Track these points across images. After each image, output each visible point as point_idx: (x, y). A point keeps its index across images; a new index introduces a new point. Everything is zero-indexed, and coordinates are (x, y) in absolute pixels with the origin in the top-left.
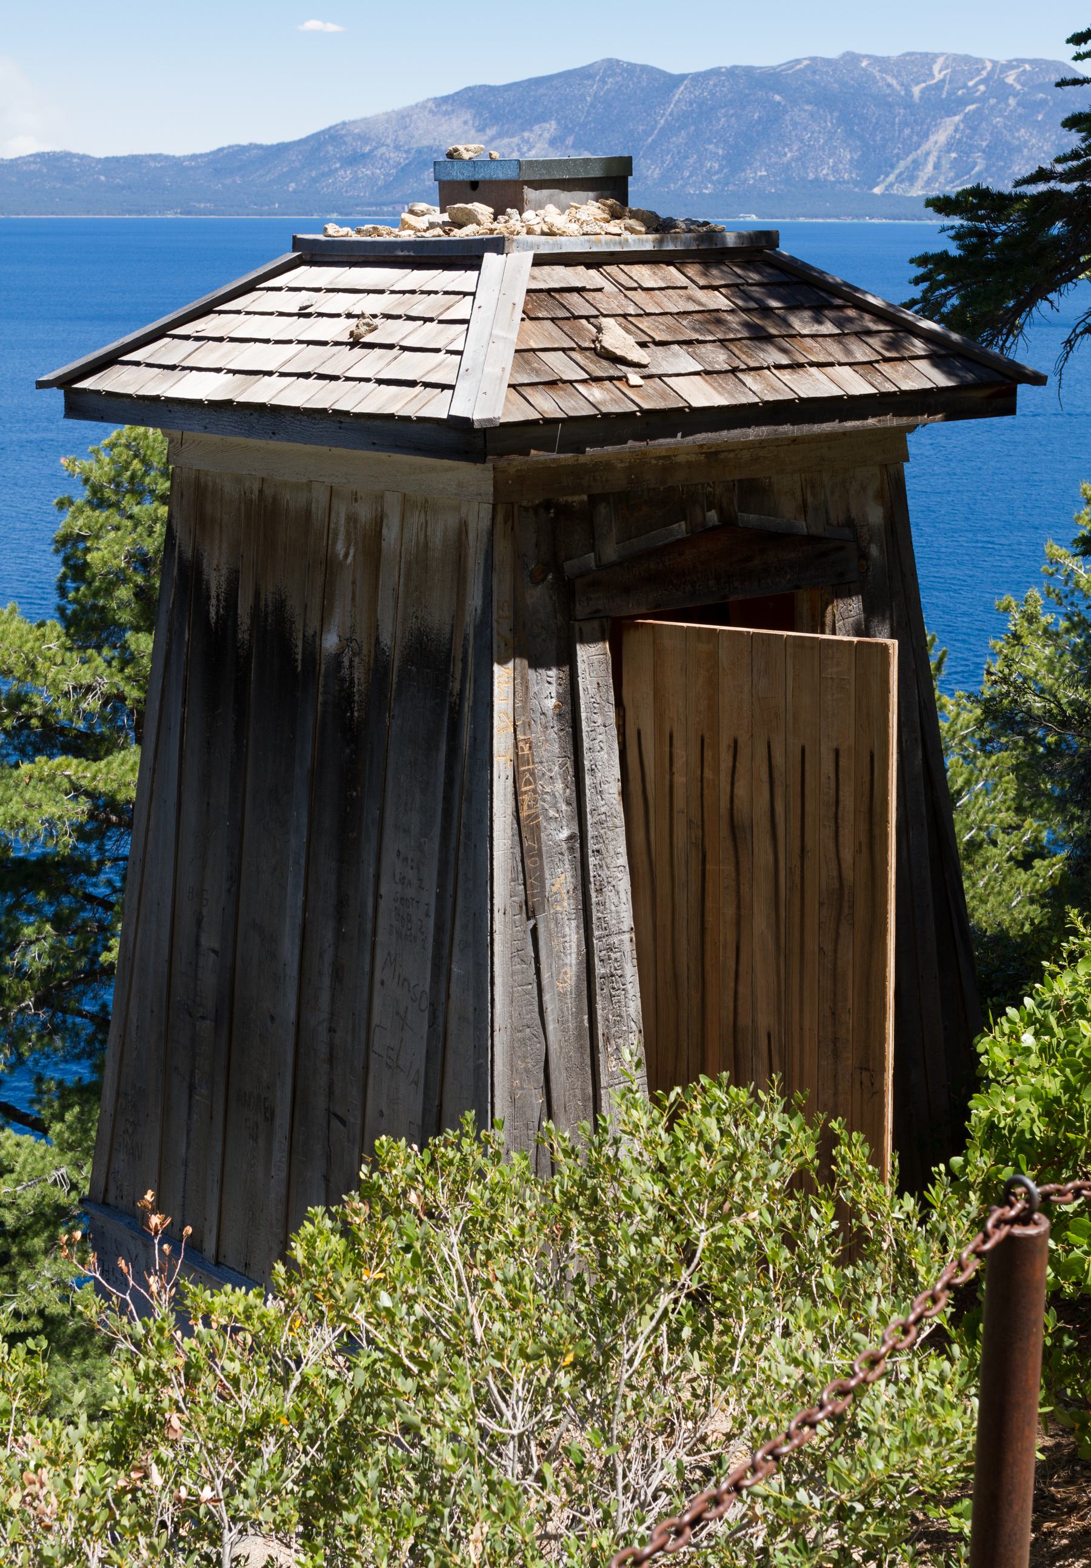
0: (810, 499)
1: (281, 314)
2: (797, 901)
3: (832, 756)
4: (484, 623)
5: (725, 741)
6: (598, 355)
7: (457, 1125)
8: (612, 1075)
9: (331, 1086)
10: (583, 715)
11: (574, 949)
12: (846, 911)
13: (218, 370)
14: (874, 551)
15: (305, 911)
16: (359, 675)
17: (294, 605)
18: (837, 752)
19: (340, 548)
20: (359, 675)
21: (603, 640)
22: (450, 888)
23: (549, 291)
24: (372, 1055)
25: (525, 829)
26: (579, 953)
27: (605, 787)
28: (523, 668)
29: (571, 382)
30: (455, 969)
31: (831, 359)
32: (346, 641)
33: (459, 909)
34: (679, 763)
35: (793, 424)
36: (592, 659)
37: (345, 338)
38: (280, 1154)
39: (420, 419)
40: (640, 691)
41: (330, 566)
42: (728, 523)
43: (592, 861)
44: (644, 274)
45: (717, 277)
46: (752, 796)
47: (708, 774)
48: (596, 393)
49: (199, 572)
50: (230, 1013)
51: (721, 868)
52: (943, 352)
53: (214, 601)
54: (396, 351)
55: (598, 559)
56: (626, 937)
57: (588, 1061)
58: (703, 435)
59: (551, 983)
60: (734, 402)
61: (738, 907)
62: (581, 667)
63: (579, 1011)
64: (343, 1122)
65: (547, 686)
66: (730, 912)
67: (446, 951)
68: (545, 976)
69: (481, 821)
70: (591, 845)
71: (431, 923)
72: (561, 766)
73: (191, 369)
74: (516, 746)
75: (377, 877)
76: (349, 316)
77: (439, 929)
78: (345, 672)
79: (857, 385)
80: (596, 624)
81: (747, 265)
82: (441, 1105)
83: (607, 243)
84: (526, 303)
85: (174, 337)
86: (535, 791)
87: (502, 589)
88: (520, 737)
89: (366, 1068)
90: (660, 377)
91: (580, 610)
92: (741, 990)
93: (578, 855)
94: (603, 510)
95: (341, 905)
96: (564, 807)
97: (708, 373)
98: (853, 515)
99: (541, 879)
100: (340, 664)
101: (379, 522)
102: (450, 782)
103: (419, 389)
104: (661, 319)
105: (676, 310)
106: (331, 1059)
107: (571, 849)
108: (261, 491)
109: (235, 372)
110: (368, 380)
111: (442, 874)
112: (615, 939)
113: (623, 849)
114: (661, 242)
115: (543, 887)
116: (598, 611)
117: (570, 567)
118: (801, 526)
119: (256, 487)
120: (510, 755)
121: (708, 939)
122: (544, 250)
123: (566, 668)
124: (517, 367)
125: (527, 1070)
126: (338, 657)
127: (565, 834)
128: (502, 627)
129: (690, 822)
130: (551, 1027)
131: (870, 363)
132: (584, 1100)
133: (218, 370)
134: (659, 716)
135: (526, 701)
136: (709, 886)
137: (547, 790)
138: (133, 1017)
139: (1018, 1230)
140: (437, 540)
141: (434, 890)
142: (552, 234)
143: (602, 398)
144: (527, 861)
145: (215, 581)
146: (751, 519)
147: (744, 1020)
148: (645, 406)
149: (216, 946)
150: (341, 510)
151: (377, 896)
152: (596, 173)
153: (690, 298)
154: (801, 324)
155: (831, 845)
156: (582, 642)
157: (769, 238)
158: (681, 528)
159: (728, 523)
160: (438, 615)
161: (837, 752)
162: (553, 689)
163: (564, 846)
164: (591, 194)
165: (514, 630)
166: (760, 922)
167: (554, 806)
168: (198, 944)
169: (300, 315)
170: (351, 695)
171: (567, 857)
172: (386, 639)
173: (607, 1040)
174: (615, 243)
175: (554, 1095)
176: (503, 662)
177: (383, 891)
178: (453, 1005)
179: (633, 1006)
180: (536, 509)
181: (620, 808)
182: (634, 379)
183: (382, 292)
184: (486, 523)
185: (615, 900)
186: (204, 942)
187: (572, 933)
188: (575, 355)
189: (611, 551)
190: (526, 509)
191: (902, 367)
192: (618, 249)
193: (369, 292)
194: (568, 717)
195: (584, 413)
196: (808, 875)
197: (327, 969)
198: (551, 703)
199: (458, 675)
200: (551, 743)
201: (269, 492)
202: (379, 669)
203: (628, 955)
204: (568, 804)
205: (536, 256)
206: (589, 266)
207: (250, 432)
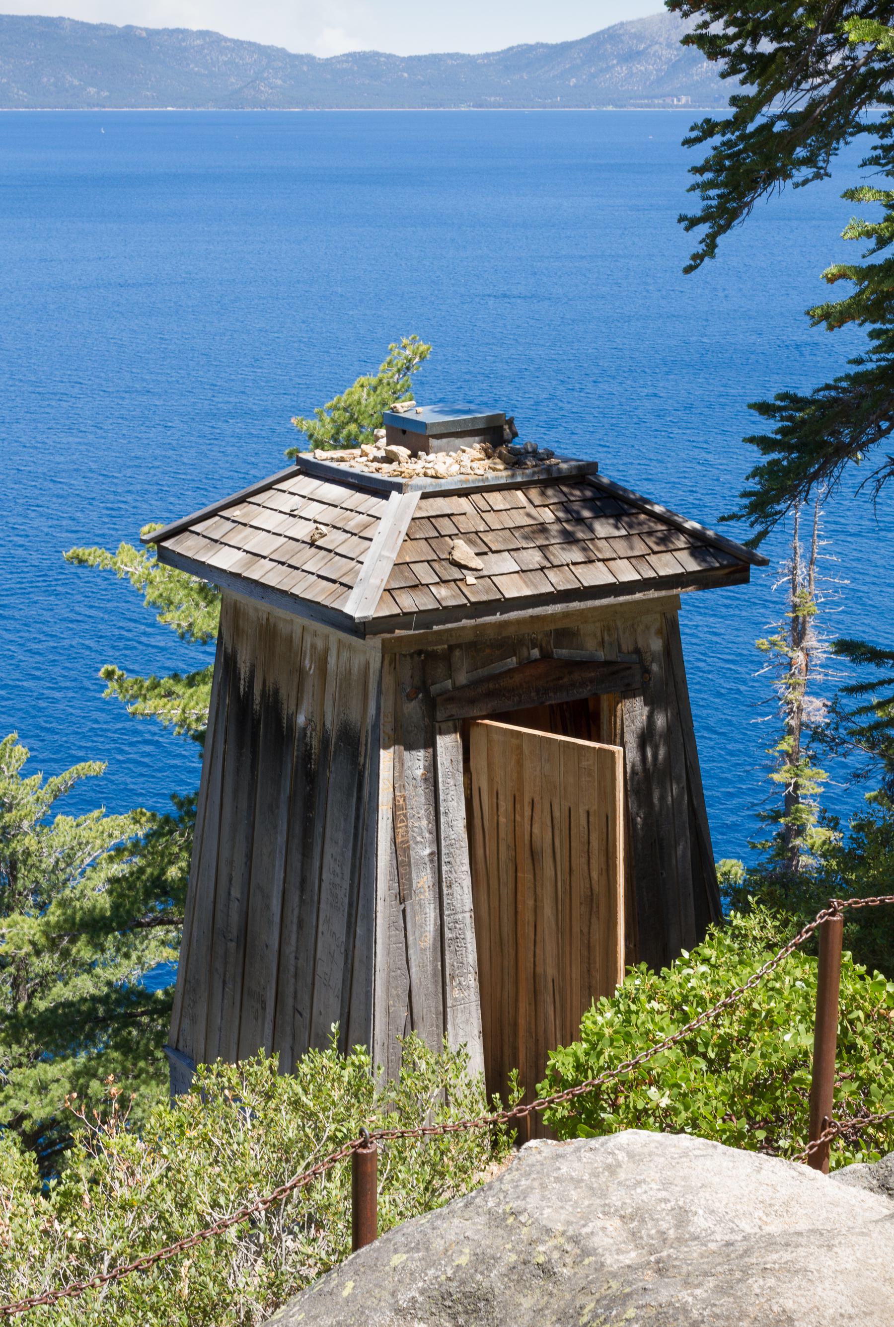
0: (606, 638)
1: (281, 512)
2: (568, 901)
3: (585, 815)
4: (376, 726)
5: (527, 800)
6: (451, 563)
7: (255, 1054)
8: (455, 999)
9: (296, 992)
10: (440, 780)
11: (432, 922)
12: (595, 909)
13: (239, 549)
14: (655, 667)
15: (284, 882)
16: (315, 743)
17: (283, 692)
18: (588, 813)
19: (307, 663)
20: (315, 743)
21: (455, 732)
22: (356, 881)
23: (428, 518)
24: (317, 977)
25: (400, 849)
26: (435, 924)
27: (454, 823)
28: (400, 752)
29: (427, 585)
30: (358, 931)
31: (615, 556)
32: (309, 721)
33: (361, 894)
34: (502, 810)
35: (580, 601)
36: (448, 745)
37: (308, 540)
38: (268, 1030)
39: (333, 608)
40: (479, 762)
41: (301, 672)
42: (546, 656)
43: (444, 868)
44: (497, 500)
45: (552, 496)
46: (542, 834)
47: (518, 818)
48: (442, 592)
49: (235, 663)
50: (245, 938)
51: (526, 876)
52: (699, 544)
53: (242, 682)
54: (332, 554)
55: (454, 683)
56: (468, 915)
57: (440, 990)
58: (515, 613)
59: (415, 944)
60: (536, 592)
61: (535, 900)
62: (439, 750)
63: (435, 959)
64: (301, 1015)
65: (417, 761)
66: (531, 903)
67: (353, 920)
68: (411, 939)
69: (372, 844)
70: (444, 858)
71: (346, 900)
72: (426, 810)
73: (226, 544)
74: (394, 799)
75: (321, 868)
76: (315, 522)
77: (350, 905)
78: (308, 739)
79: (627, 574)
80: (450, 724)
81: (573, 486)
82: (349, 1012)
83: (473, 481)
84: (410, 528)
85: (222, 517)
86: (407, 826)
87: (388, 705)
88: (397, 794)
89: (313, 984)
90: (489, 577)
91: (440, 716)
92: (537, 951)
93: (436, 864)
94: (457, 653)
95: (303, 881)
96: (427, 835)
97: (523, 571)
98: (640, 645)
99: (410, 880)
100: (305, 734)
101: (326, 651)
102: (357, 818)
103: (337, 585)
104: (500, 533)
105: (512, 525)
106: (296, 975)
107: (432, 861)
108: (268, 619)
109: (248, 552)
110: (313, 574)
111: (352, 873)
112: (460, 916)
113: (466, 861)
114: (513, 476)
115: (411, 884)
116: (452, 716)
117: (434, 689)
118: (601, 655)
119: (265, 616)
120: (390, 805)
121: (519, 918)
122: (430, 490)
123: (430, 750)
124: (392, 575)
125: (398, 996)
126: (305, 729)
127: (428, 851)
128: (387, 727)
129: (508, 846)
130: (413, 970)
131: (643, 556)
132: (437, 1014)
133: (239, 549)
134: (491, 780)
135: (402, 771)
136: (519, 885)
137: (416, 825)
138: (195, 934)
139: (360, 1151)
140: (355, 670)
141: (349, 882)
142: (437, 477)
143: (446, 595)
144: (400, 869)
145: (244, 670)
146: (563, 653)
147: (539, 970)
148: (473, 600)
149: (239, 896)
150: (308, 640)
151: (321, 880)
152: (481, 426)
153: (529, 515)
154: (603, 528)
155: (586, 868)
156: (440, 734)
157: (592, 467)
158: (512, 662)
159: (546, 656)
160: (354, 715)
161: (588, 813)
162: (421, 764)
163: (427, 859)
164: (477, 439)
165: (395, 730)
166: (548, 911)
167: (421, 834)
168: (229, 894)
169: (291, 515)
170: (311, 754)
171: (429, 866)
172: (328, 725)
173: (453, 978)
174: (479, 481)
175: (415, 1011)
176: (386, 747)
177: (324, 877)
178: (356, 952)
179: (471, 957)
180: (411, 655)
181: (465, 836)
182: (471, 580)
183: (336, 506)
184: (378, 665)
185: (460, 892)
186: (232, 893)
187: (431, 913)
188: (436, 565)
189: (462, 678)
190: (405, 656)
191: (668, 557)
192: (481, 484)
193: (330, 505)
194: (431, 780)
195: (430, 607)
196: (573, 885)
197: (295, 920)
198: (419, 772)
199: (363, 754)
200: (418, 799)
201: (272, 620)
202: (325, 742)
203: (469, 926)
204: (430, 833)
205: (423, 494)
206: (460, 496)
207: (251, 594)
